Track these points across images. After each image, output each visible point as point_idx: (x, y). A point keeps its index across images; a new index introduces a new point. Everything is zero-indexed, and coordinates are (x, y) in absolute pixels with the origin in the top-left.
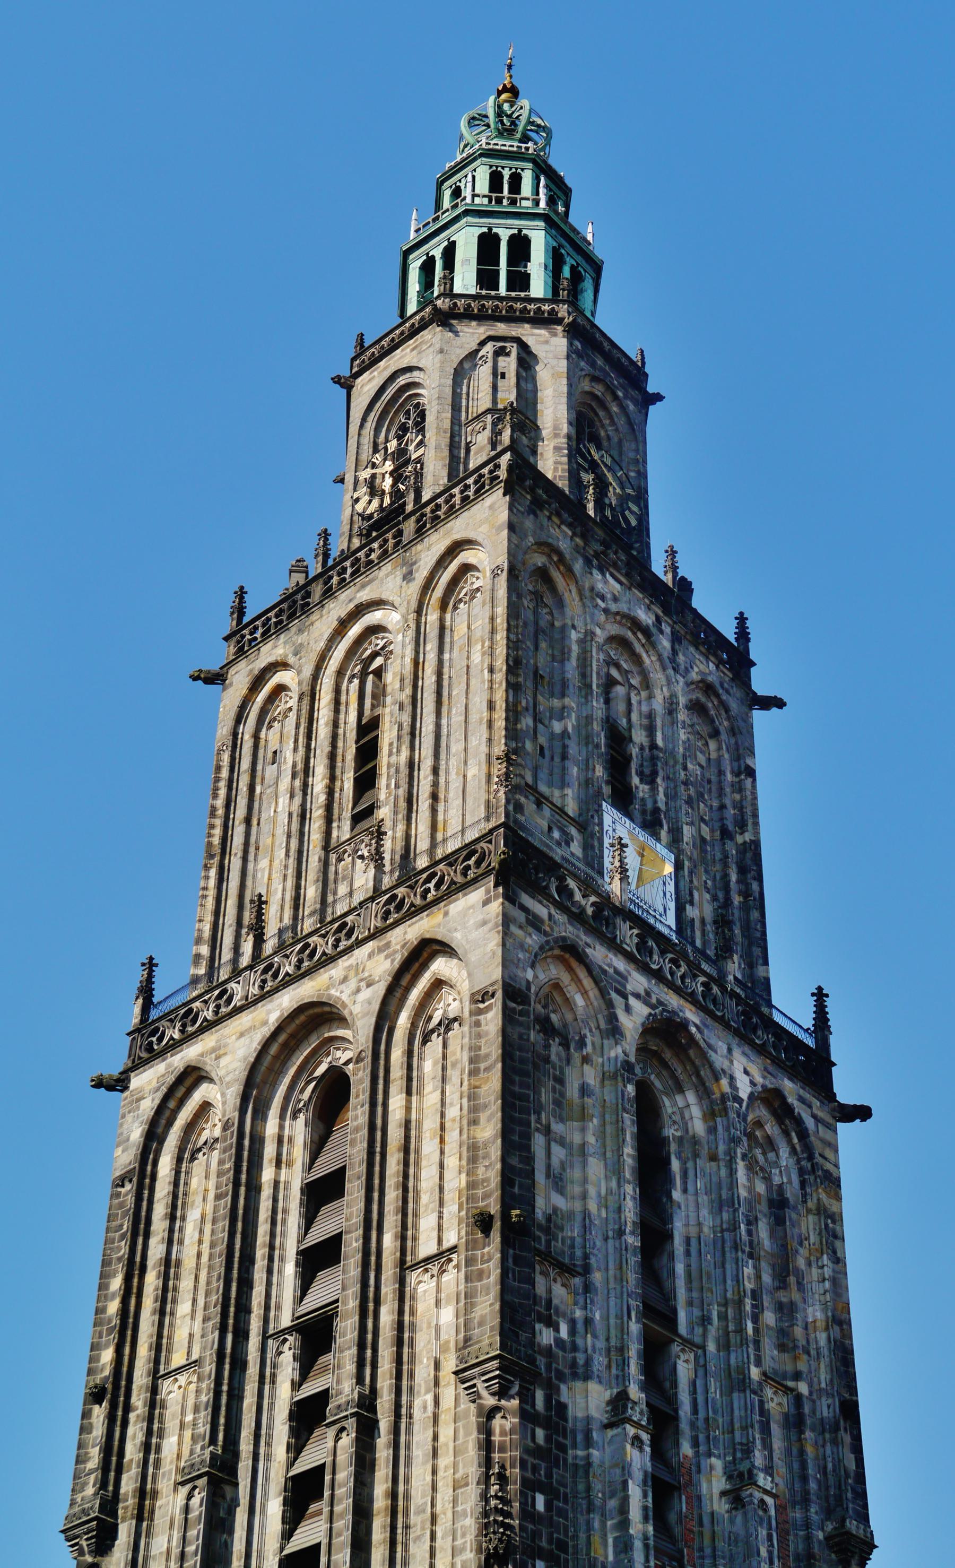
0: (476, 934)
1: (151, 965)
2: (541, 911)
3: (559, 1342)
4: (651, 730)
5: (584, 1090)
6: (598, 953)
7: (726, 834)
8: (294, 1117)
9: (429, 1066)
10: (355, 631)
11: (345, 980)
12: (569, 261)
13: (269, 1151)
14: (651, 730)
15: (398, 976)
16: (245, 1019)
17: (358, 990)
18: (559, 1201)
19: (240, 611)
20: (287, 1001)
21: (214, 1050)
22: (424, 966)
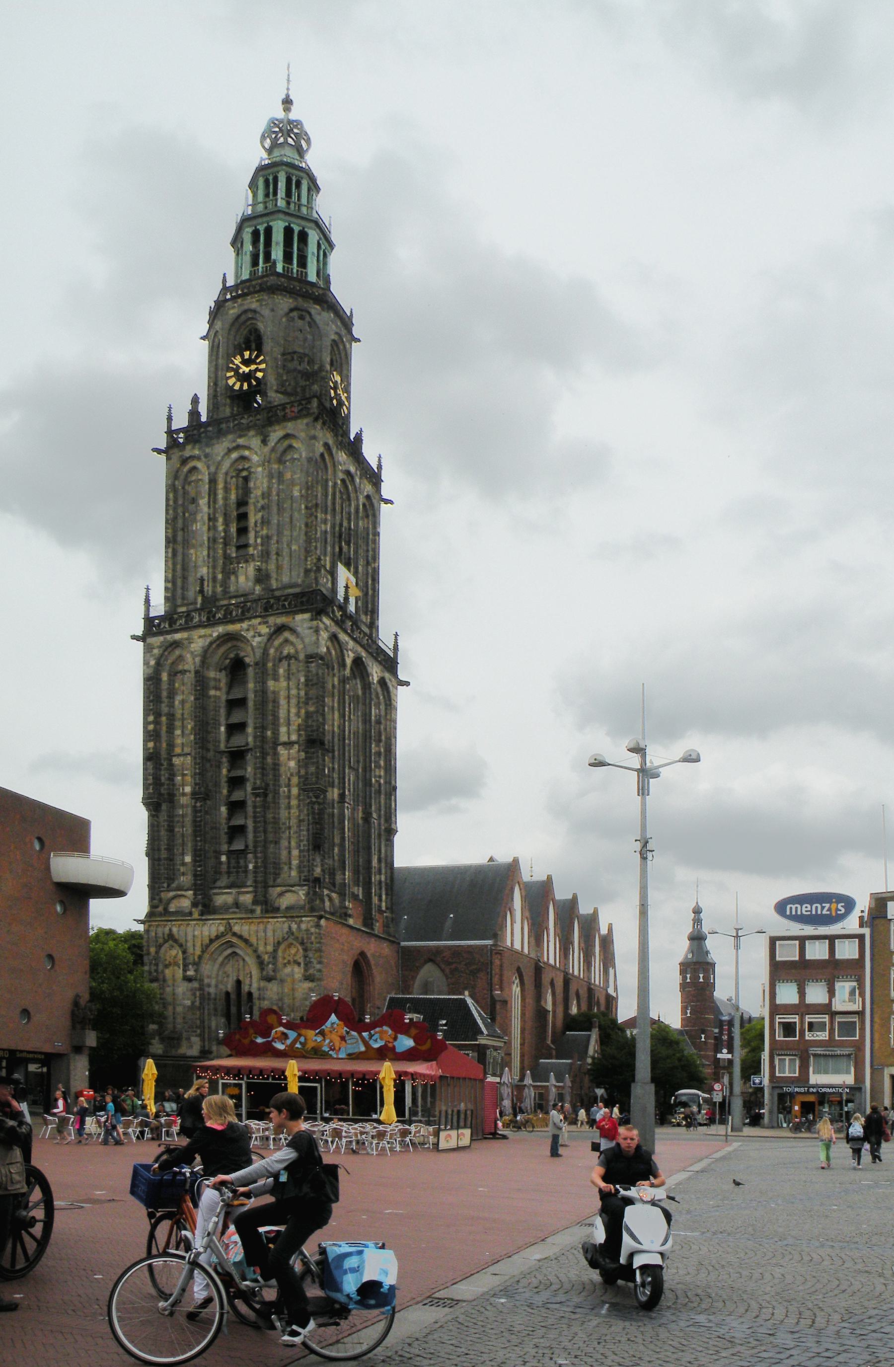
0: (307, 632)
1: (148, 589)
8: (220, 671)
9: (281, 671)
10: (234, 455)
11: (248, 630)
13: (212, 684)
16: (202, 632)
17: (254, 636)
19: (170, 419)
20: (221, 629)
21: (187, 639)
22: (281, 633)
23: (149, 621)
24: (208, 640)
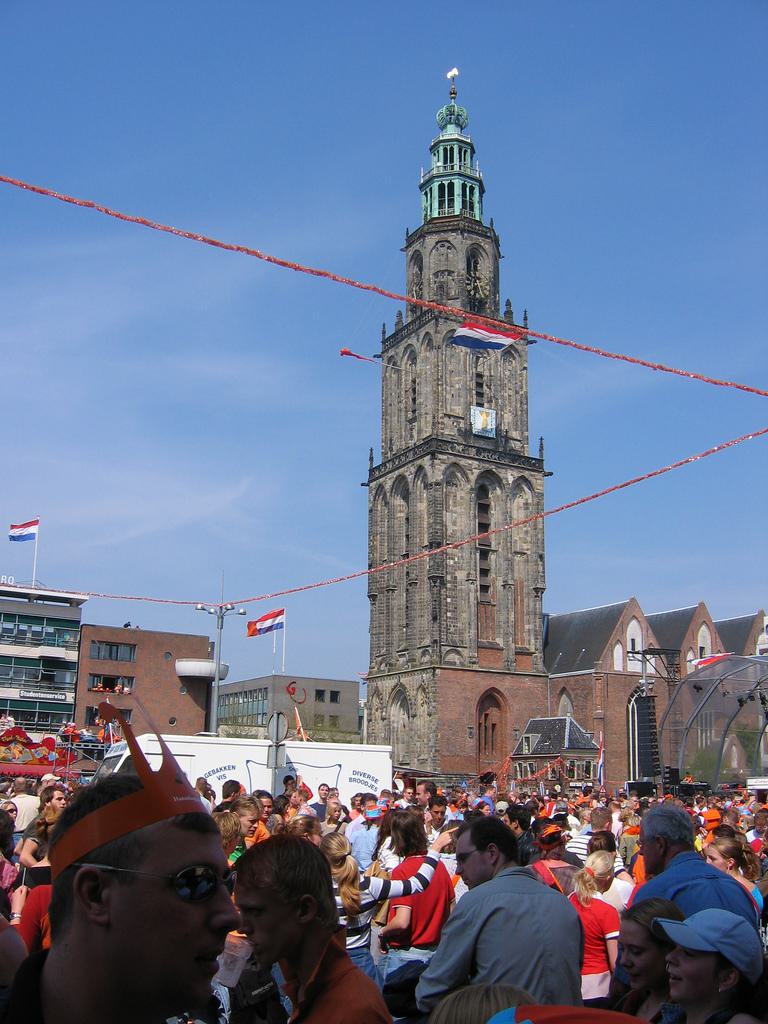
2: (445, 457)
3: (455, 563)
4: (490, 370)
5: (462, 498)
6: (463, 462)
7: (517, 392)
12: (469, 185)
14: (490, 370)
15: (416, 473)
18: (455, 528)
19: (384, 333)
23: (372, 471)
24: (393, 480)
